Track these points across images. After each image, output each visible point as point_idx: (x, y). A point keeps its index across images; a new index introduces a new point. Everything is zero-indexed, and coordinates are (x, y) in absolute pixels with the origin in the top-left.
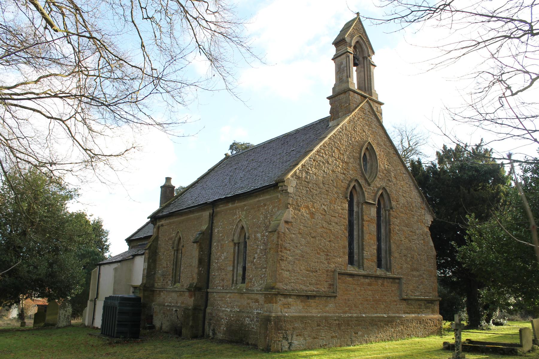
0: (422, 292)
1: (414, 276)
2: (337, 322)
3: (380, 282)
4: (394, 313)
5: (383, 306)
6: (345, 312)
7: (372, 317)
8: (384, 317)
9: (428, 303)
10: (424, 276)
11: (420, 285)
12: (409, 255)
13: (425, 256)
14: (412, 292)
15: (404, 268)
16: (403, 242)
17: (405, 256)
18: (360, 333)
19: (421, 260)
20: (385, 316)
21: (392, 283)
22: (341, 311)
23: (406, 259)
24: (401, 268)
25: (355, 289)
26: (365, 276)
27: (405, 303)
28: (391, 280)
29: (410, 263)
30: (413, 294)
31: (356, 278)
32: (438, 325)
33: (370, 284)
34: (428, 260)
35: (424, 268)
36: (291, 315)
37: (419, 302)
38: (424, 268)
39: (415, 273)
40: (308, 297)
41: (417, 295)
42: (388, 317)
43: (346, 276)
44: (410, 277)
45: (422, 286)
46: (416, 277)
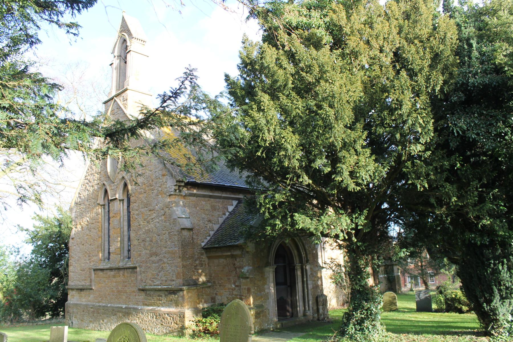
0: (162, 280)
1: (153, 262)
2: (92, 310)
3: (121, 272)
4: (134, 305)
5: (124, 297)
6: (99, 302)
7: (113, 307)
8: (122, 307)
9: (170, 293)
10: (165, 260)
11: (160, 272)
12: (148, 239)
13: (167, 235)
14: (152, 281)
15: (142, 254)
16: (141, 226)
17: (143, 241)
18: (105, 321)
19: (161, 241)
20: (124, 306)
21: (131, 273)
22: (97, 301)
23: (144, 244)
24: (140, 255)
25: (105, 282)
26: (111, 269)
27: (143, 294)
28: (131, 270)
29: (149, 248)
30: (153, 284)
31: (105, 272)
32: (178, 322)
33: (114, 276)
34: (170, 239)
35: (164, 250)
36: (73, 302)
37: (159, 293)
38: (164, 250)
39: (154, 258)
40: (81, 290)
41: (157, 284)
42: (126, 308)
43: (99, 271)
44: (148, 264)
45: (162, 272)
46: (155, 263)
